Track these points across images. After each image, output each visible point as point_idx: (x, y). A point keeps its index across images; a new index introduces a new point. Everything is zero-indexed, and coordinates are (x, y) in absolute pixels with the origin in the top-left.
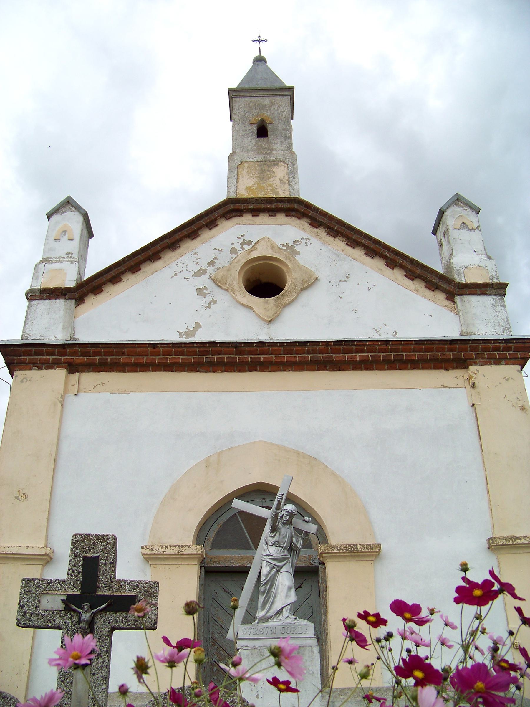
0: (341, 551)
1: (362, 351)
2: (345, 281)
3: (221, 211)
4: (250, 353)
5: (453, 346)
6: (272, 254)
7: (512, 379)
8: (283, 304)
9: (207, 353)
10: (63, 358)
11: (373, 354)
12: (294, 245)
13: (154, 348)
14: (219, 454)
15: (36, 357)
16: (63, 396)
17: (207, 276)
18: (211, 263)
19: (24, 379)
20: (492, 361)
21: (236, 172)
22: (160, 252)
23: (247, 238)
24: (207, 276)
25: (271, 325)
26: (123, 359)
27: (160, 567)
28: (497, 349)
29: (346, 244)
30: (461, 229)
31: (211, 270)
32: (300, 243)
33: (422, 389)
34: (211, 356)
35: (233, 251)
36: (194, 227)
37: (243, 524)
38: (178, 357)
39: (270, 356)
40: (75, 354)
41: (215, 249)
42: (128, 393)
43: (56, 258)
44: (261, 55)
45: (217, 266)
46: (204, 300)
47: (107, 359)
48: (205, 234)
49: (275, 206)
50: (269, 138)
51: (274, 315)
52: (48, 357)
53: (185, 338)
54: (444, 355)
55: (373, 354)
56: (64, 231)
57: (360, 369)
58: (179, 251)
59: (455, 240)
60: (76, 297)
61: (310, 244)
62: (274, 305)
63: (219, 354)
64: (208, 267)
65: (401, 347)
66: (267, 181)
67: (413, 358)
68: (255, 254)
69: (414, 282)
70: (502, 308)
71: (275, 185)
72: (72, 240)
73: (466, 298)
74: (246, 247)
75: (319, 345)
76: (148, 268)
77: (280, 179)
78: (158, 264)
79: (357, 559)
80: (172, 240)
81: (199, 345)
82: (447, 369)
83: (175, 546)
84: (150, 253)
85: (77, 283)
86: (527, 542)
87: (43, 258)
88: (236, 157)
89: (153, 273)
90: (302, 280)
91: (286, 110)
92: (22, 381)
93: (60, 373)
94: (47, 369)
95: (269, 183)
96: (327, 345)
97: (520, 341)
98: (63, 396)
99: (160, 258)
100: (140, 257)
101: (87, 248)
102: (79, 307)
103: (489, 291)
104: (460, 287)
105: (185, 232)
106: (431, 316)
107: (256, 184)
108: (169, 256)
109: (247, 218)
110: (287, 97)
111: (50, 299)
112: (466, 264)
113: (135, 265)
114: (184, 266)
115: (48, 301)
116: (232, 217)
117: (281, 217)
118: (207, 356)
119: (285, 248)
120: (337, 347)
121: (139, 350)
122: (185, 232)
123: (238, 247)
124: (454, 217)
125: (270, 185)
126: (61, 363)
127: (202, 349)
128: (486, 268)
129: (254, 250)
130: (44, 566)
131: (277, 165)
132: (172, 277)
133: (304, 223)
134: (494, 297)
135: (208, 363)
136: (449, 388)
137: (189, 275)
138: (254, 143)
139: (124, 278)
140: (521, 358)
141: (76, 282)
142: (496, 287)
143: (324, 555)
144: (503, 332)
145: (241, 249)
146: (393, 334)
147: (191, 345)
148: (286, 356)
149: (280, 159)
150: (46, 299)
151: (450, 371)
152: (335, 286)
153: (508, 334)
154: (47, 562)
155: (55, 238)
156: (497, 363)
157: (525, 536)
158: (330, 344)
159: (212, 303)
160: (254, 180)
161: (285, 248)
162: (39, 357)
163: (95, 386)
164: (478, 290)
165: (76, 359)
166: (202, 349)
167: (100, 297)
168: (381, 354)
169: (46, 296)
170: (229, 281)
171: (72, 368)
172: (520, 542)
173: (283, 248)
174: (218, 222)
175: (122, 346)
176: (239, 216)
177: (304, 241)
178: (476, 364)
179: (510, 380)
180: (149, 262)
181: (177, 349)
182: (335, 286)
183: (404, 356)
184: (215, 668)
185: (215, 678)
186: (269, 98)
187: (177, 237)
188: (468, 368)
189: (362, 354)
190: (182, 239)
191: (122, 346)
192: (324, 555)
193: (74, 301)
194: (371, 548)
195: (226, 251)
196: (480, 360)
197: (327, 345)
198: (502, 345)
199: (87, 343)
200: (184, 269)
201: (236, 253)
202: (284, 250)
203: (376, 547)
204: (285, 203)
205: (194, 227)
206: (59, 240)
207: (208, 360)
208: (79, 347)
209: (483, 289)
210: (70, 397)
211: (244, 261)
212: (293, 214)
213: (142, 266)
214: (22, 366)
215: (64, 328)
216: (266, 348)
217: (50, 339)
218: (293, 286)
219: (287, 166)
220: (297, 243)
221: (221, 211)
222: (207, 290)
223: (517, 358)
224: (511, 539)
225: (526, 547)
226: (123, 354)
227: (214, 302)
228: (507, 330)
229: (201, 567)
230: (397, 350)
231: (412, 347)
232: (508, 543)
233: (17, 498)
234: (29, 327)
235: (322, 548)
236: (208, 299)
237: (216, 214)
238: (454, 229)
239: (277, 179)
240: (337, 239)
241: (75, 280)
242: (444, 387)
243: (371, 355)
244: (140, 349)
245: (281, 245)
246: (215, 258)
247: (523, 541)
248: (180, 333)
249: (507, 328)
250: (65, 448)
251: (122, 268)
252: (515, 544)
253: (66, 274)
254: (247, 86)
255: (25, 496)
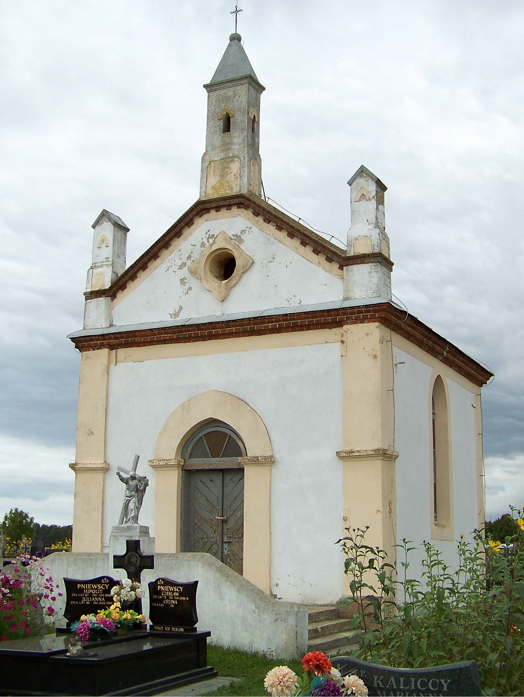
0: (250, 461)
1: (272, 322)
2: (272, 261)
3: (194, 213)
4: (206, 329)
5: (330, 313)
6: (226, 246)
7: (371, 334)
8: (230, 287)
9: (182, 331)
10: (105, 342)
11: (279, 323)
12: (241, 235)
13: (152, 331)
14: (189, 400)
15: (91, 342)
16: (108, 368)
17: (186, 268)
18: (189, 257)
19: (87, 357)
20: (359, 320)
21: (206, 173)
22: (158, 252)
23: (211, 233)
24: (186, 268)
25: (223, 303)
26: (137, 339)
27: (159, 472)
28: (361, 312)
29: (276, 228)
30: (360, 201)
31: (189, 263)
32: (245, 233)
33: (311, 345)
34: (185, 333)
35: (203, 245)
36: (177, 229)
37: (207, 443)
38: (166, 335)
39: (218, 330)
40: (110, 339)
41: (192, 245)
42: (142, 361)
43: (100, 263)
44: (237, 33)
45: (192, 259)
46: (185, 287)
47: (129, 340)
48: (187, 232)
49: (228, 202)
50: (231, 133)
51: (224, 296)
52: (97, 342)
53: (174, 318)
54: (325, 319)
55: (279, 323)
56: (102, 240)
57: (274, 333)
58: (171, 248)
59: (354, 212)
60: (111, 295)
61: (252, 232)
62: (225, 288)
63: (189, 332)
64: (187, 260)
65: (296, 317)
66: (226, 178)
67: (304, 324)
68: (215, 247)
69: (319, 256)
70: (375, 273)
71: (231, 181)
72: (108, 247)
73: (351, 267)
74: (211, 241)
75: (244, 321)
76: (152, 265)
77: (235, 175)
78: (159, 260)
79: (260, 465)
80: (164, 242)
81: (176, 327)
82: (330, 328)
83: (164, 460)
84: (151, 254)
85: (112, 283)
86: (358, 455)
87: (93, 264)
88: (207, 157)
89: (155, 269)
90: (242, 265)
91: (244, 100)
92: (86, 359)
93: (105, 351)
94: (98, 350)
95: (228, 180)
96: (250, 320)
97: (376, 305)
98: (108, 368)
99: (159, 256)
100: (146, 259)
101: (125, 243)
102: (114, 301)
103: (367, 260)
104: (346, 260)
105: (172, 234)
106: (326, 285)
107: (219, 182)
108: (165, 253)
109: (213, 213)
110: (245, 85)
111: (96, 298)
112: (357, 236)
113: (143, 265)
114: (173, 261)
115: (96, 299)
116: (203, 215)
117: (235, 209)
118: (182, 333)
119: (235, 238)
120: (256, 321)
121: (144, 333)
122: (172, 234)
123: (205, 241)
124: (357, 190)
125: (228, 182)
126: (104, 345)
127: (178, 330)
128: (371, 238)
129: (214, 243)
130: (105, 473)
131: (233, 161)
132: (166, 271)
133: (249, 213)
134: (371, 264)
135: (183, 338)
136: (330, 343)
137: (175, 268)
138: (220, 139)
139: (139, 275)
140: (378, 317)
141: (111, 282)
142: (372, 257)
143: (242, 463)
144: (372, 295)
145: (208, 243)
146: (299, 303)
147: (171, 328)
148: (227, 329)
149: (236, 154)
150: (94, 298)
151: (332, 329)
152: (265, 267)
153: (375, 296)
154: (107, 471)
155: (99, 247)
156: (362, 322)
157: (357, 451)
158: (251, 319)
159: (189, 290)
160: (218, 178)
161: (235, 238)
162: (93, 342)
163: (125, 358)
164: (359, 261)
165: (113, 342)
166: (178, 330)
167: (126, 291)
168: (284, 323)
169: (94, 296)
170: (198, 272)
171: (112, 347)
172: (354, 454)
173: (234, 238)
174: (195, 221)
175: (134, 332)
176: (208, 213)
177: (248, 230)
178: (347, 324)
179: (370, 335)
180: (153, 260)
181: (164, 331)
182: (265, 267)
183: (299, 323)
184: (196, 527)
185: (196, 532)
186: (233, 89)
187: (167, 239)
188: (343, 326)
189: (273, 324)
190: (171, 239)
191: (134, 332)
192: (242, 463)
193: (110, 298)
194: (266, 459)
195: (199, 245)
196: (350, 321)
197: (250, 320)
198: (363, 309)
199: (115, 332)
200: (173, 265)
201: (204, 246)
202: (234, 239)
203: (269, 458)
204: (235, 199)
205: (177, 229)
206: (101, 247)
207: (184, 336)
208: (112, 335)
209: (363, 259)
210: (112, 366)
211: (208, 254)
212: (242, 206)
213: (149, 265)
214: (84, 349)
215: (106, 319)
216: (214, 326)
217: (99, 327)
218: (237, 272)
219: (240, 161)
220: (243, 233)
221: (194, 213)
222: (186, 279)
223: (376, 318)
224: (349, 452)
225: (358, 457)
226: (136, 337)
227: (190, 288)
228: (376, 292)
229: (182, 470)
230: (294, 319)
231: (303, 316)
232: (346, 455)
233: (89, 434)
234: (86, 320)
235: (240, 459)
236: (187, 286)
237: (191, 216)
238: (355, 202)
239: (233, 174)
240: (270, 225)
241: (110, 280)
242: (327, 342)
243: (278, 324)
244: (144, 333)
245: (233, 236)
246: (192, 253)
247: (356, 454)
248: (171, 315)
249: (376, 291)
250: (112, 401)
251: (135, 269)
252: (351, 456)
253: (105, 276)
254: (221, 79)
255: (92, 433)
